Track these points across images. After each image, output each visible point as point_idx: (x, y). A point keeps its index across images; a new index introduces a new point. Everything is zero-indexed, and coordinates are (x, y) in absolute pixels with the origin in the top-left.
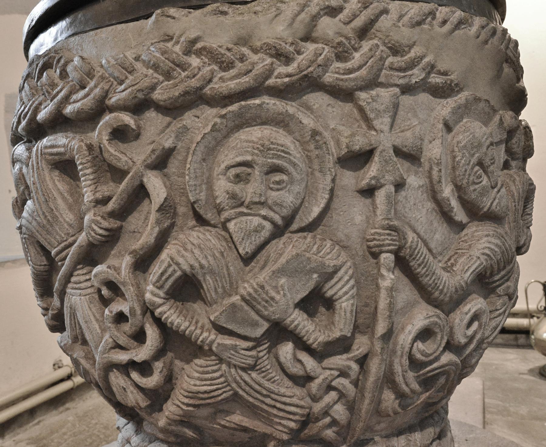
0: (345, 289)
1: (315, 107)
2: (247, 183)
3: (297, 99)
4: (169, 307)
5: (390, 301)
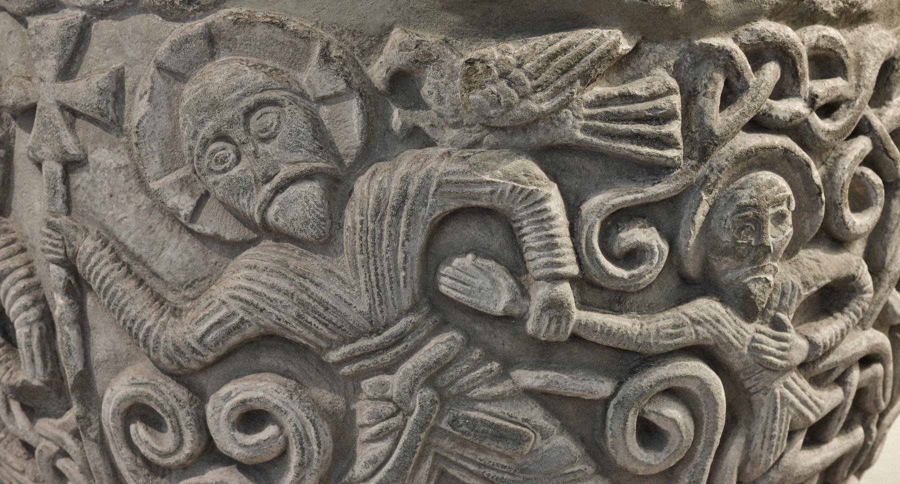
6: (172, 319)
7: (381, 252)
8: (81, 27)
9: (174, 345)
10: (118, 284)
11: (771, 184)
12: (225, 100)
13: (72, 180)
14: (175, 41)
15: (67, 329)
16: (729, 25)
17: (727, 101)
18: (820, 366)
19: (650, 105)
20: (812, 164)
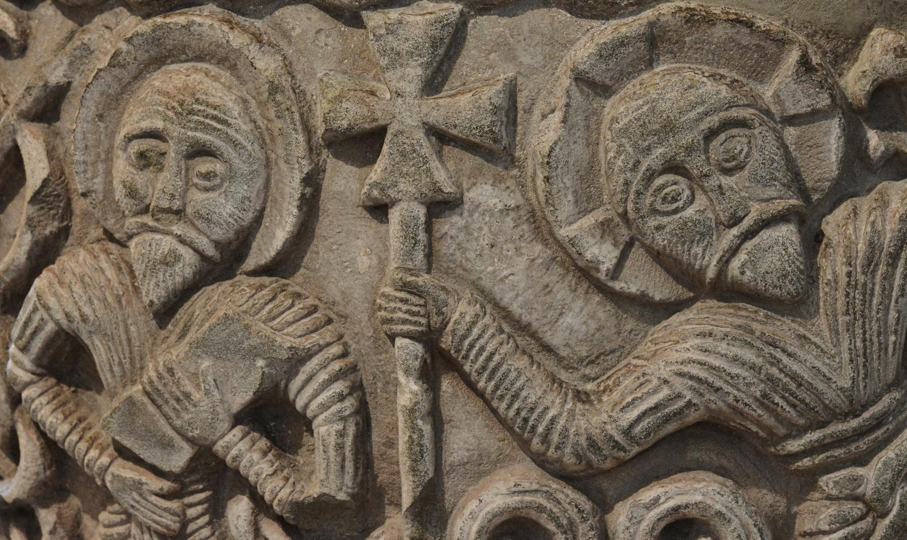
0: (321, 399)
1: (294, 34)
2: (161, 170)
3: (266, 14)
4: (39, 391)
5: (410, 437)
6: (580, 406)
7: (870, 312)
8: (457, 25)
9: (589, 438)
10: (510, 362)
12: (682, 120)
13: (436, 227)
14: (605, 43)
15: (420, 422)
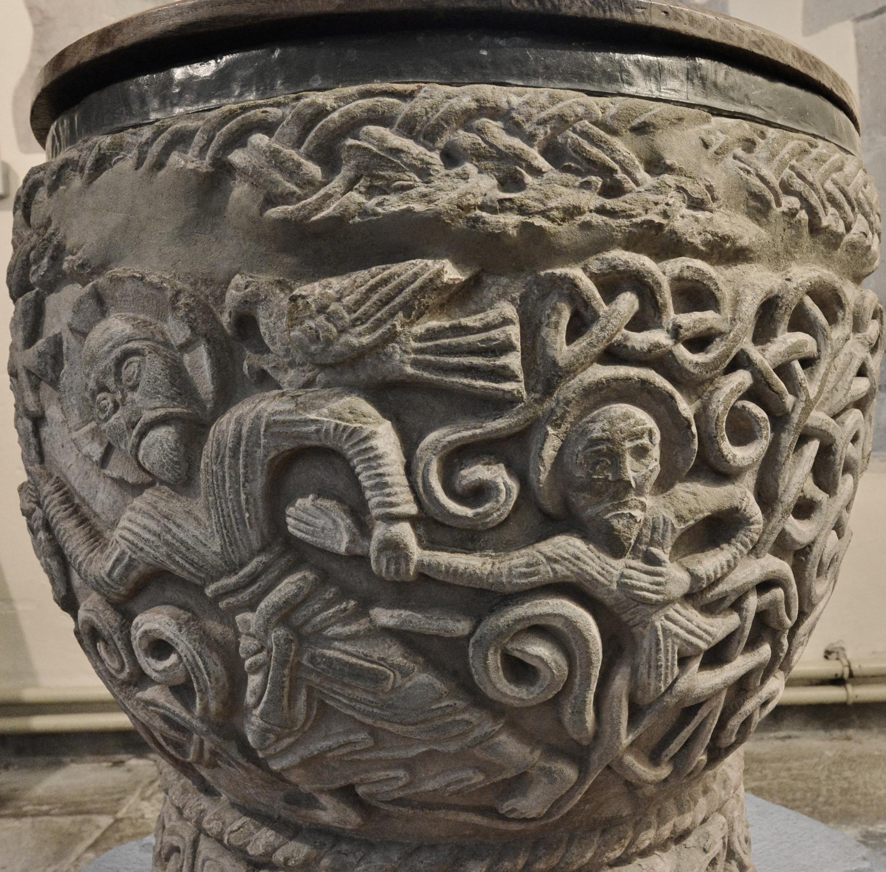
7: (225, 494)
11: (626, 417)
16: (578, 255)
17: (575, 331)
18: (709, 596)
19: (483, 336)
20: (678, 396)
